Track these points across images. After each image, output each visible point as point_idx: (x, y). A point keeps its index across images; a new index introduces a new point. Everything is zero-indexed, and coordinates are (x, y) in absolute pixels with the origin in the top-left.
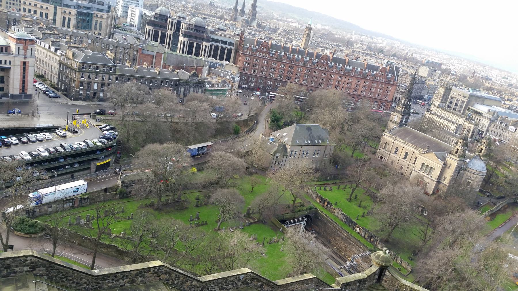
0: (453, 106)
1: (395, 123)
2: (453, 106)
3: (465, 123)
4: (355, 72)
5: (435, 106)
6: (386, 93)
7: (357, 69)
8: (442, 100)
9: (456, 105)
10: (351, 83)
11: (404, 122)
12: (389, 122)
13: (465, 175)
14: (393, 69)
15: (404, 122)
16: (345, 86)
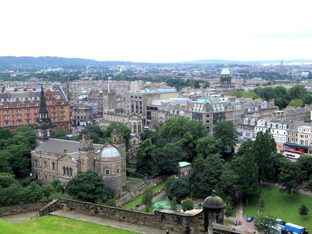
0: (135, 109)
1: (40, 139)
2: (135, 109)
3: (130, 121)
4: (20, 102)
5: (105, 114)
6: (61, 115)
7: (22, 99)
8: (109, 106)
9: (137, 107)
10: (20, 115)
11: (48, 135)
12: (37, 140)
13: (102, 166)
14: (60, 90)
15: (48, 135)
16: (15, 120)
